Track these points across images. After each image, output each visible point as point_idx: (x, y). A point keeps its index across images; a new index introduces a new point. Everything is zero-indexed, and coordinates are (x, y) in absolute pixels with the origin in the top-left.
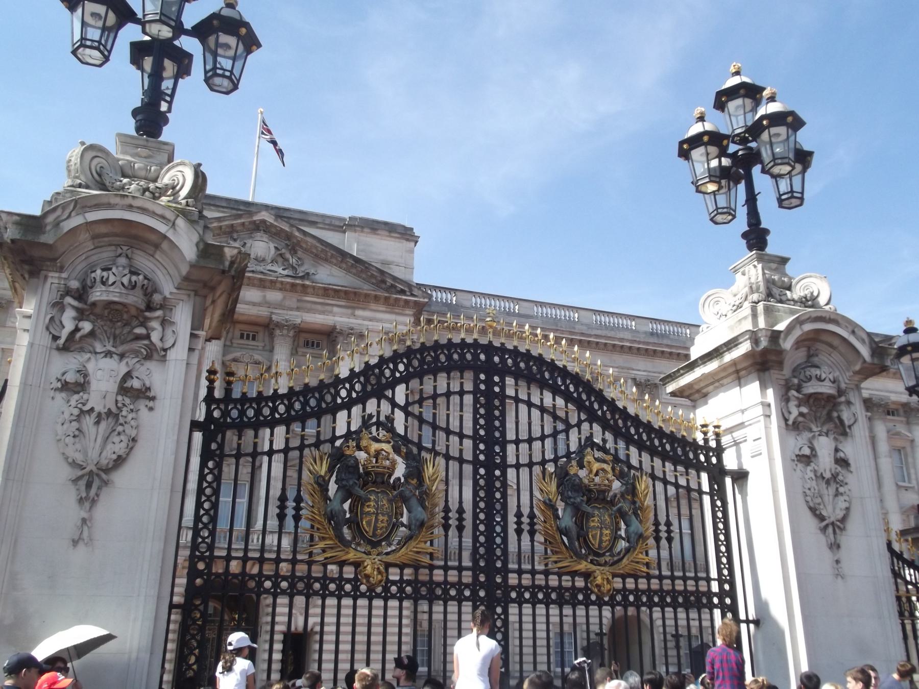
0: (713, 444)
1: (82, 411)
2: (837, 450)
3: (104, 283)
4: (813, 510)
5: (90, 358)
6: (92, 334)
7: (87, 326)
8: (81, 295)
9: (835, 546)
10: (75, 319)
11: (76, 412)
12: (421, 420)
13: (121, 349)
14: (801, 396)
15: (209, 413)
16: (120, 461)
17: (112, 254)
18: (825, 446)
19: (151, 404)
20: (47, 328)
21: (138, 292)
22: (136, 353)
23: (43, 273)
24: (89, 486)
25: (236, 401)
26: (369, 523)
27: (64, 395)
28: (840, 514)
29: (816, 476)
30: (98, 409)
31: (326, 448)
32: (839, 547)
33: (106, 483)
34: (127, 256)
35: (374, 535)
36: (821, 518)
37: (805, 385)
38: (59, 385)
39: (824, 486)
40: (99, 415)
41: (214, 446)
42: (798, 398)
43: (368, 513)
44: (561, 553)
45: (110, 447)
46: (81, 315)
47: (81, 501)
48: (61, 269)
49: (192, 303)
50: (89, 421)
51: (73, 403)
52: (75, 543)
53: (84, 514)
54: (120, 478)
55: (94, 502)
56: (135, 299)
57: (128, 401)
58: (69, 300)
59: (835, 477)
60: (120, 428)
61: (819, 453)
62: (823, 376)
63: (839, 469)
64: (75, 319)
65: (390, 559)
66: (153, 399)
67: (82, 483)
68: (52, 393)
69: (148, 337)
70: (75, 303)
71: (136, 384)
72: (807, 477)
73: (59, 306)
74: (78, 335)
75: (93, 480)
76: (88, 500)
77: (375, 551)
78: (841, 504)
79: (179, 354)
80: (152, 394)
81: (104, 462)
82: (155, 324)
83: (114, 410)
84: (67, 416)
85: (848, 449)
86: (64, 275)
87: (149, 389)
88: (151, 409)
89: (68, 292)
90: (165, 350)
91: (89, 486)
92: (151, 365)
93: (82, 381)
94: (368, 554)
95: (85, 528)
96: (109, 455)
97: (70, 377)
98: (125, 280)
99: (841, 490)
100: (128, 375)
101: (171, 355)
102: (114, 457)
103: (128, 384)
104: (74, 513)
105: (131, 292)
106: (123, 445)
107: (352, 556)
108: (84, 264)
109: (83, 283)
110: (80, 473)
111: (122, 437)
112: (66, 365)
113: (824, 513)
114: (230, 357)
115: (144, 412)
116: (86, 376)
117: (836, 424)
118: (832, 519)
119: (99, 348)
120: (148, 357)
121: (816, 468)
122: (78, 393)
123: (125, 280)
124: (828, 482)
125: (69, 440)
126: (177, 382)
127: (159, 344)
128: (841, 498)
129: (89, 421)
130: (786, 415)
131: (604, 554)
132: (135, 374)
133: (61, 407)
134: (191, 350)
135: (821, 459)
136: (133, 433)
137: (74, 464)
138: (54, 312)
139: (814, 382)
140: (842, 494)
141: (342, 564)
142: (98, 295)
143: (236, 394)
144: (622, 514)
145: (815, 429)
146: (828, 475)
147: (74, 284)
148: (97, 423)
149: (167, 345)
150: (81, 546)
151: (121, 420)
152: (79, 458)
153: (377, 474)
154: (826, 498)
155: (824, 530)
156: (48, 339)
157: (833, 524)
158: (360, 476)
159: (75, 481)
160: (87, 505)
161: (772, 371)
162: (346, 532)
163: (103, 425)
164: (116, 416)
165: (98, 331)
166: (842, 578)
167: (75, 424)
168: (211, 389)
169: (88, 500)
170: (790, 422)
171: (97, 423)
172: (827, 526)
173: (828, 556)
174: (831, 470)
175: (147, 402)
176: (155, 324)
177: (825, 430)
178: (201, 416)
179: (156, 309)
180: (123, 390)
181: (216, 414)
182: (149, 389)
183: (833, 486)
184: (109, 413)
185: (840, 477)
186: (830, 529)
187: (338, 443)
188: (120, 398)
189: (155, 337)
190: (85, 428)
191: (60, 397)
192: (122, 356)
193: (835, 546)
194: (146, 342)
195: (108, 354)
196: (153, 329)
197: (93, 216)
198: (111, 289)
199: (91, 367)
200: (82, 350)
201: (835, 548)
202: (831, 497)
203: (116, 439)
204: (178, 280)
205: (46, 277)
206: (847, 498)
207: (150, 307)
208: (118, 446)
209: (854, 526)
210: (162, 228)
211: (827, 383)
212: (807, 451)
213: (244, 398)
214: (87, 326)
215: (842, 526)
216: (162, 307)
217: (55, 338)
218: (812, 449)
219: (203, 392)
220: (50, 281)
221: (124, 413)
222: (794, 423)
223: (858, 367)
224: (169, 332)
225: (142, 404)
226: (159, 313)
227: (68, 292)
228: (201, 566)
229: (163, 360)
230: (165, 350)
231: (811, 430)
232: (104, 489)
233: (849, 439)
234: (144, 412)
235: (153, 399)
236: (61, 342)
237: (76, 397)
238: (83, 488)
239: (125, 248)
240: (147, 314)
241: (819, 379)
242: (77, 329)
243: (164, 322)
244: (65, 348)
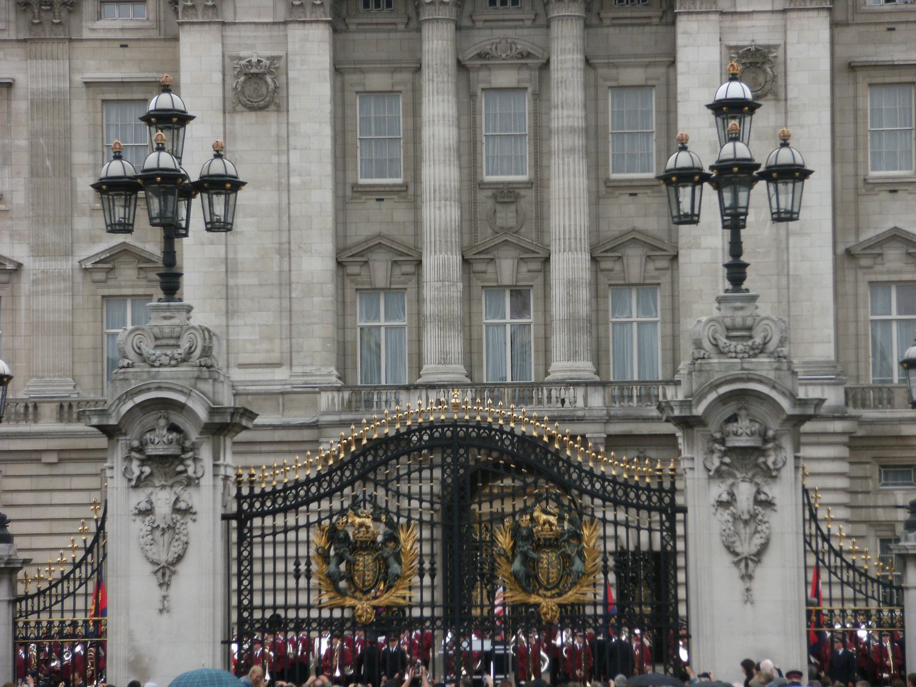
0: (667, 485)
1: (153, 528)
2: (758, 492)
3: (153, 443)
4: (728, 548)
5: (152, 493)
6: (151, 474)
7: (147, 470)
8: (140, 450)
9: (747, 577)
10: (139, 466)
11: (149, 528)
12: (398, 494)
13: (170, 482)
14: (723, 448)
15: (240, 506)
16: (179, 558)
17: (155, 416)
18: (745, 492)
19: (194, 517)
20: (124, 475)
21: (174, 445)
22: (180, 483)
23: (116, 438)
24: (164, 575)
25: (258, 496)
26: (359, 578)
27: (141, 517)
28: (754, 549)
29: (735, 519)
30: (162, 525)
31: (326, 523)
32: (750, 577)
33: (174, 573)
34: (165, 417)
35: (364, 586)
36: (736, 554)
37: (727, 439)
38: (137, 511)
39: (742, 526)
40: (163, 529)
41: (246, 531)
42: (720, 451)
43: (357, 570)
44: (516, 590)
45: (172, 549)
46: (143, 463)
47: (161, 585)
48: (125, 434)
49: (211, 443)
50: (158, 533)
51: (147, 523)
52: (161, 611)
53: (163, 593)
54: (181, 568)
55: (168, 585)
56: (173, 450)
57: (179, 517)
58: (134, 454)
59: (753, 516)
60: (177, 537)
61: (738, 498)
62: (740, 431)
63: (760, 509)
64: (139, 466)
65: (375, 602)
66: (195, 513)
67: (160, 574)
68: (134, 517)
69: (185, 471)
70: (138, 456)
71: (182, 505)
72: (723, 520)
73: (128, 459)
74: (143, 477)
75: (165, 573)
76: (164, 584)
77: (365, 598)
78: (758, 540)
79: (207, 481)
80: (193, 510)
81: (170, 560)
82: (189, 462)
83: (171, 524)
84: (144, 530)
85: (773, 491)
86: (128, 437)
87: (191, 508)
88: (194, 520)
89: (132, 449)
90: (198, 479)
91: (164, 575)
92: (191, 490)
93: (149, 507)
94: (361, 600)
95: (166, 602)
96: (171, 557)
97: (143, 506)
98: (165, 439)
99: (759, 528)
100: (177, 500)
101: (203, 482)
102: (176, 555)
103: (177, 507)
104: (158, 593)
105: (170, 446)
106: (180, 547)
107: (349, 602)
108: (139, 427)
109: (141, 444)
110: (157, 568)
111: (179, 542)
112: (139, 498)
113: (738, 550)
114: (472, 52)
115: (190, 525)
116: (151, 503)
117: (761, 468)
118: (744, 555)
119: (157, 483)
120: (188, 485)
121: (734, 511)
122: (148, 515)
123: (165, 439)
124: (746, 522)
125: (148, 547)
126: (208, 500)
127: (194, 476)
128: (758, 535)
129: (158, 533)
130: (709, 465)
131: (553, 588)
132: (181, 499)
133: (140, 526)
134: (215, 475)
135: (739, 504)
136: (185, 539)
137: (153, 563)
138: (125, 464)
139: (732, 437)
140: (759, 532)
141: (343, 608)
142: (151, 451)
143: (257, 490)
144: (569, 556)
145: (738, 475)
146: (746, 516)
147: (136, 443)
148: (163, 534)
149: (199, 474)
150: (165, 612)
151: (177, 531)
152: (156, 558)
153: (361, 542)
154: (743, 537)
155: (736, 564)
156: (126, 481)
157: (746, 558)
158: (350, 543)
159: (156, 573)
160: (165, 587)
161: (696, 429)
162: (343, 584)
163: (166, 536)
164: (174, 528)
165: (155, 471)
166: (752, 603)
167: (150, 537)
168: (239, 489)
169: (164, 584)
170: (711, 473)
171: (163, 534)
172: (741, 560)
173: (740, 586)
174: (749, 512)
175: (191, 516)
176: (189, 462)
177: (750, 475)
178: (234, 508)
179: (188, 452)
180: (176, 510)
181: (245, 506)
182: (191, 508)
183: (753, 525)
184: (169, 527)
185: (760, 517)
186: (743, 565)
187: (335, 518)
188: (174, 516)
189: (190, 471)
190: (156, 539)
191: (139, 519)
192: (172, 486)
193: (747, 577)
194: (185, 475)
195: (163, 487)
196: (189, 466)
197: (139, 399)
198: (158, 447)
199: (153, 498)
200: (146, 486)
201: (747, 579)
202: (748, 536)
203: (176, 544)
204: (200, 430)
205: (118, 440)
206: (764, 536)
207: (184, 450)
208: (176, 549)
209: (771, 558)
210: (181, 398)
211: (744, 438)
212: (725, 497)
213: (263, 494)
214: (147, 470)
215: (756, 559)
216: (192, 450)
217: (130, 480)
218: (732, 494)
219: (234, 492)
220: (120, 443)
221: (178, 526)
222: (718, 471)
223: (784, 417)
224: (198, 465)
225: (188, 518)
226: (190, 454)
227: (132, 449)
228: (246, 614)
229: (198, 485)
230: (198, 479)
231: (735, 477)
232: (174, 577)
233: (778, 480)
234: (190, 525)
235: (195, 513)
236: (133, 483)
237: (148, 518)
238: (160, 578)
239: (163, 411)
240: (183, 456)
241: (736, 434)
242: (142, 473)
243: (195, 460)
244: (136, 487)
